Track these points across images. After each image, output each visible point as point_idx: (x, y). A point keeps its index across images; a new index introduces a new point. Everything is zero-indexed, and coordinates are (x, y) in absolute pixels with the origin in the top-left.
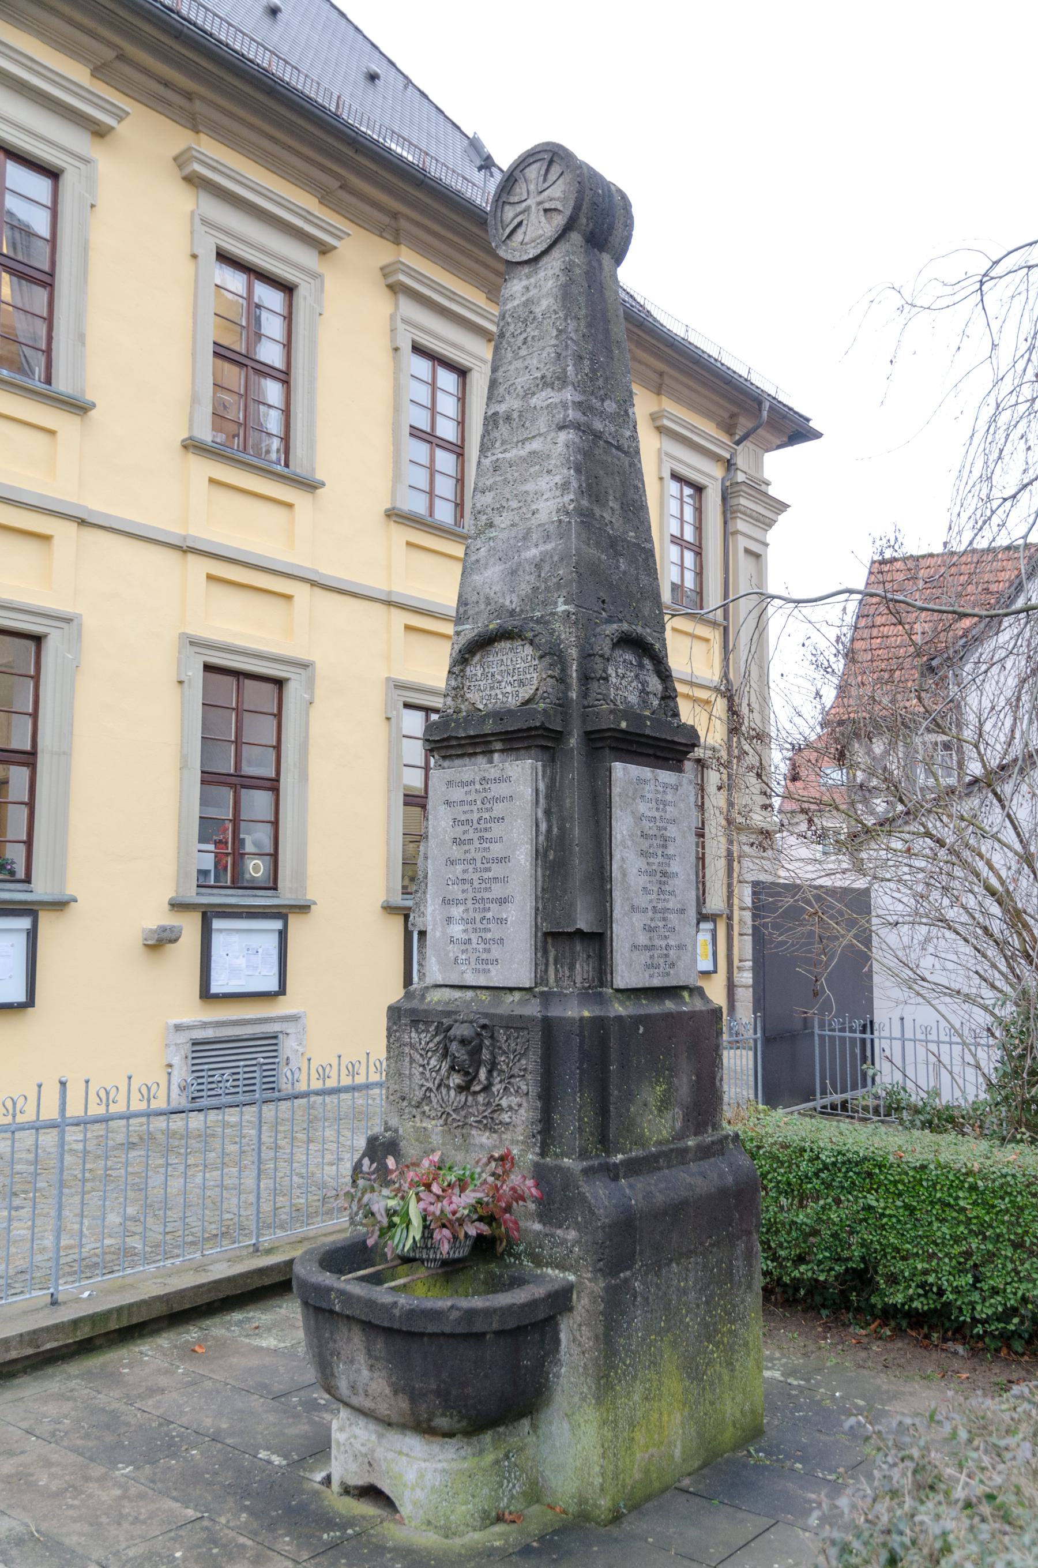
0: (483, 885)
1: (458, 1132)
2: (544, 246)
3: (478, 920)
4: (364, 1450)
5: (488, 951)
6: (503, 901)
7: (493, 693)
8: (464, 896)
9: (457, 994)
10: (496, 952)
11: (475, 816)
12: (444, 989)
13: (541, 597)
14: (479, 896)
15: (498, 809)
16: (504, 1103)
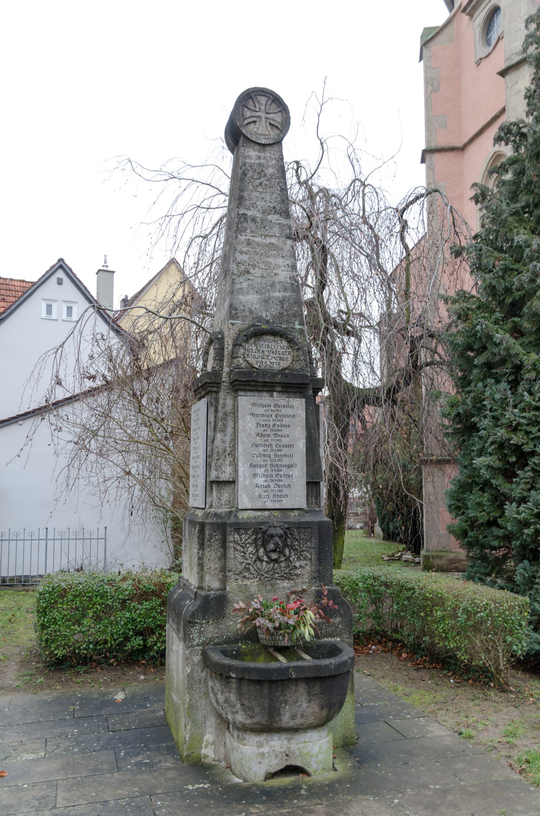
0: (277, 458)
1: (268, 583)
2: (271, 142)
3: (274, 475)
4: (282, 750)
5: (282, 491)
6: (289, 466)
7: (264, 360)
8: (265, 463)
9: (258, 513)
10: (285, 491)
11: (271, 423)
12: (249, 511)
13: (285, 318)
14: (274, 463)
15: (286, 421)
16: (297, 564)
